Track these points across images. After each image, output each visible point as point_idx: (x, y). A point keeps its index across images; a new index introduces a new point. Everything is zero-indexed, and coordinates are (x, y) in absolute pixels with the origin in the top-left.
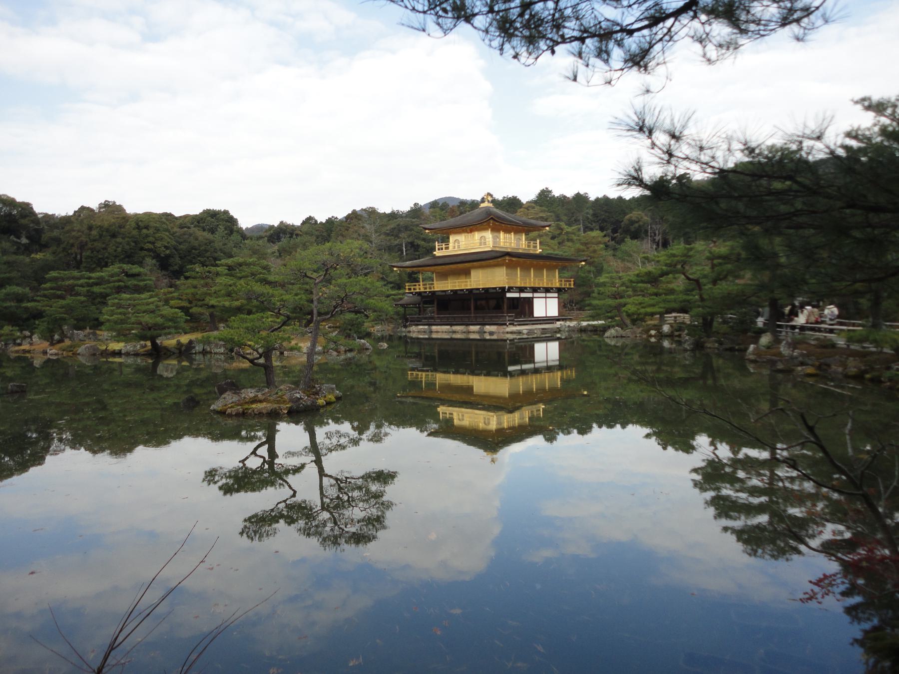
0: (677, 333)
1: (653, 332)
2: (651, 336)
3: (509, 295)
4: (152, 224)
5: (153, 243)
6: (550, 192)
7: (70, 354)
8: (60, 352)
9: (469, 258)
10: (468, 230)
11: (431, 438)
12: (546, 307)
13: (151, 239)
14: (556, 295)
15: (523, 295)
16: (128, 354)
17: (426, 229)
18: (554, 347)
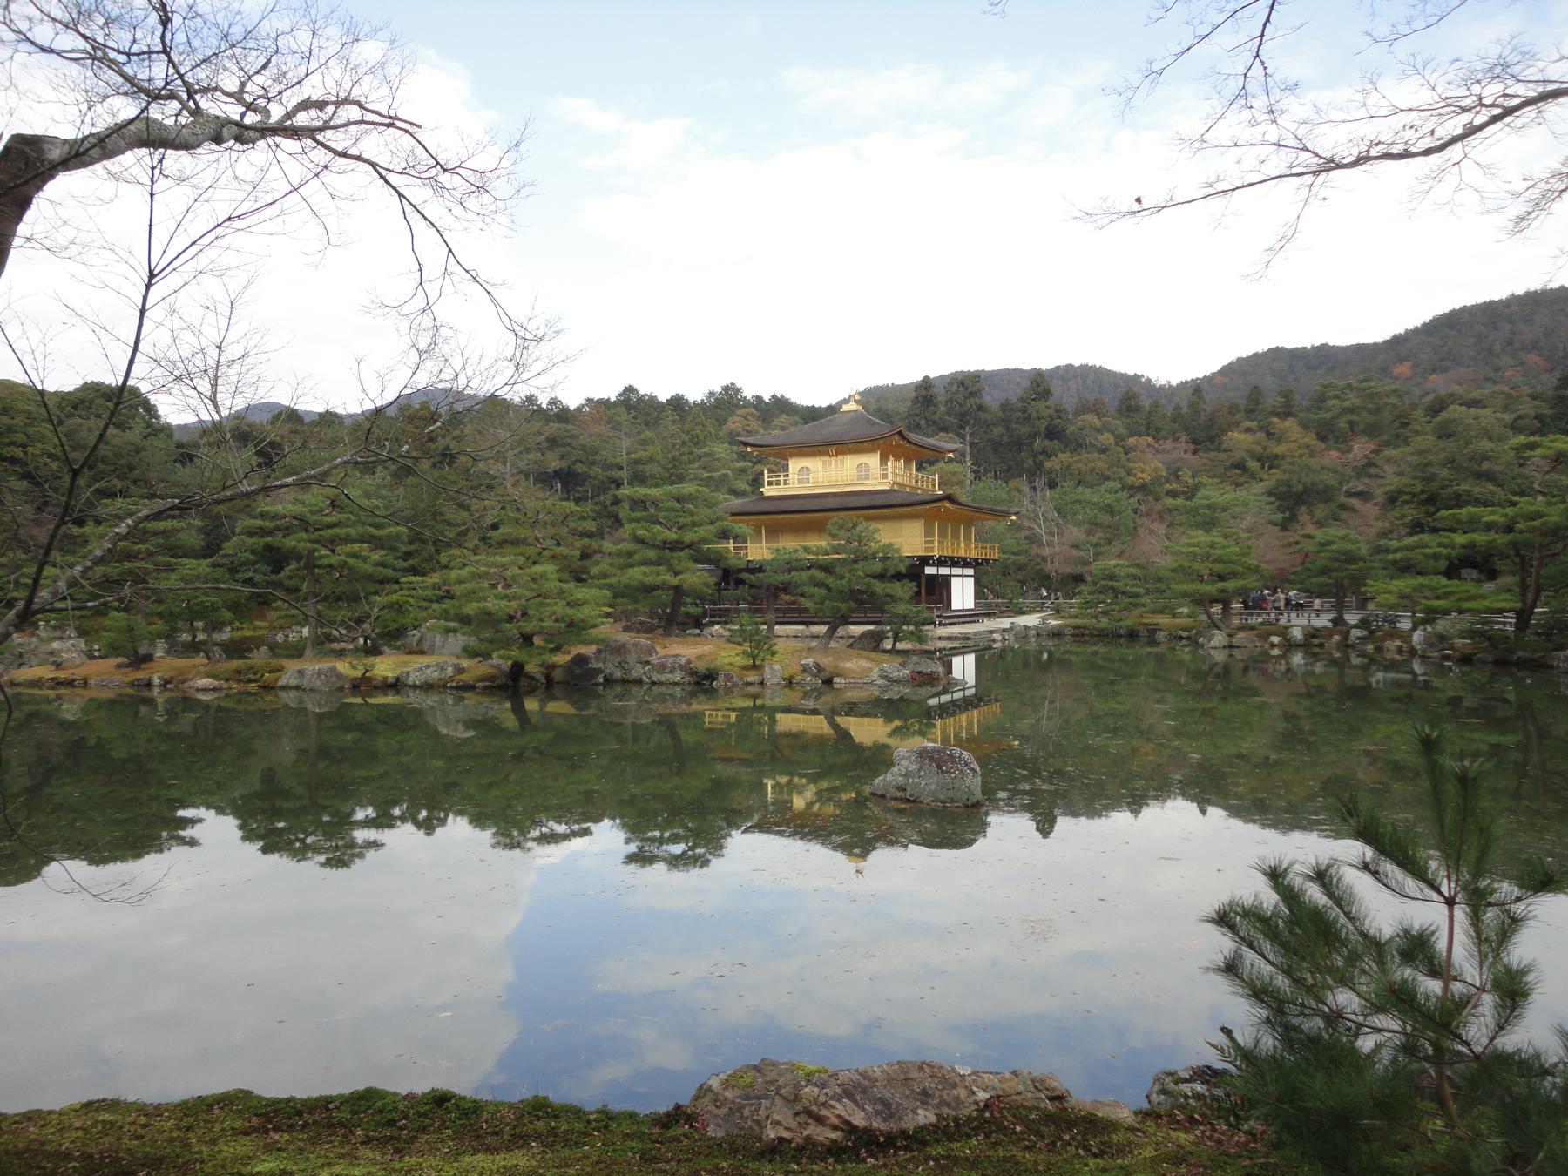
0: (1316, 641)
1: (1275, 639)
2: (1273, 646)
3: (930, 570)
4: (20, 405)
5: (24, 446)
6: (739, 390)
7: (252, 687)
8: (225, 685)
9: (853, 502)
10: (832, 450)
11: (747, 836)
12: (963, 593)
13: (20, 438)
14: (971, 571)
15: (944, 571)
16: (427, 687)
17: (746, 444)
18: (971, 659)
